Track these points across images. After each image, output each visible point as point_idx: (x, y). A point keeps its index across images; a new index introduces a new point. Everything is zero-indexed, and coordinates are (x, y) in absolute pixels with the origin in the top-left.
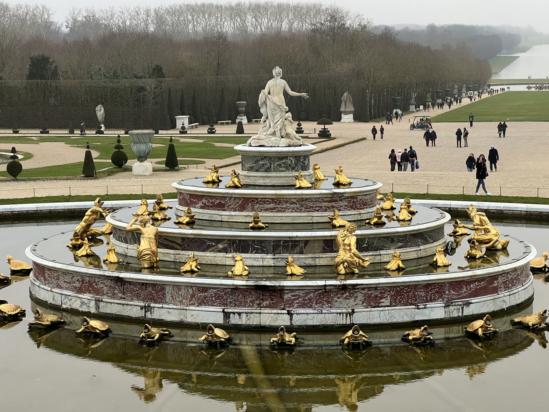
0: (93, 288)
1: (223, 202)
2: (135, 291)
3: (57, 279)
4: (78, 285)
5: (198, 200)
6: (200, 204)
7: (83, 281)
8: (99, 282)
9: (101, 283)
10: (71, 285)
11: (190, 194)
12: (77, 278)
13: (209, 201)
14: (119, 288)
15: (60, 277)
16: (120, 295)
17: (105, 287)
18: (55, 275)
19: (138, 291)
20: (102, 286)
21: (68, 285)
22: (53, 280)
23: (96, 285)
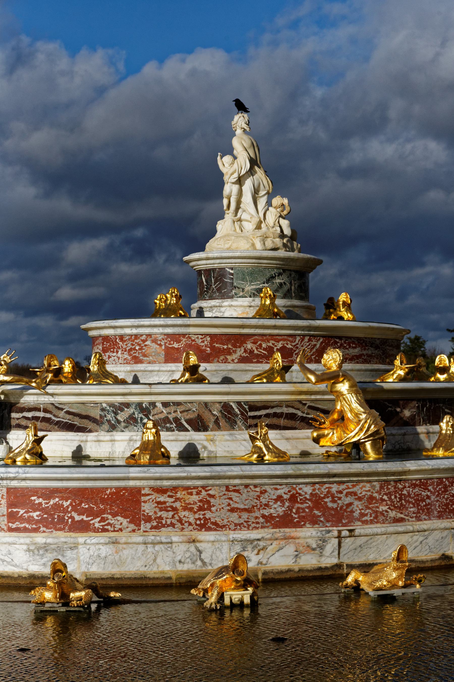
0: (325, 509)
1: (289, 346)
2: (423, 500)
3: (201, 509)
4: (277, 510)
5: (235, 346)
6: (240, 352)
7: (293, 499)
8: (341, 492)
9: (346, 496)
10: (257, 514)
11: (210, 335)
12: (274, 494)
13: (260, 345)
14: (390, 499)
15: (212, 500)
16: (392, 514)
17: (356, 503)
18: (195, 498)
19: (428, 497)
20: (348, 500)
21: (245, 515)
22: (182, 514)
23: (333, 501)
